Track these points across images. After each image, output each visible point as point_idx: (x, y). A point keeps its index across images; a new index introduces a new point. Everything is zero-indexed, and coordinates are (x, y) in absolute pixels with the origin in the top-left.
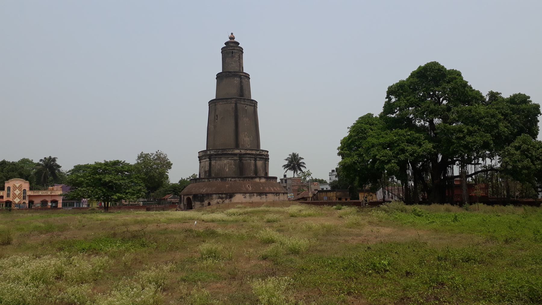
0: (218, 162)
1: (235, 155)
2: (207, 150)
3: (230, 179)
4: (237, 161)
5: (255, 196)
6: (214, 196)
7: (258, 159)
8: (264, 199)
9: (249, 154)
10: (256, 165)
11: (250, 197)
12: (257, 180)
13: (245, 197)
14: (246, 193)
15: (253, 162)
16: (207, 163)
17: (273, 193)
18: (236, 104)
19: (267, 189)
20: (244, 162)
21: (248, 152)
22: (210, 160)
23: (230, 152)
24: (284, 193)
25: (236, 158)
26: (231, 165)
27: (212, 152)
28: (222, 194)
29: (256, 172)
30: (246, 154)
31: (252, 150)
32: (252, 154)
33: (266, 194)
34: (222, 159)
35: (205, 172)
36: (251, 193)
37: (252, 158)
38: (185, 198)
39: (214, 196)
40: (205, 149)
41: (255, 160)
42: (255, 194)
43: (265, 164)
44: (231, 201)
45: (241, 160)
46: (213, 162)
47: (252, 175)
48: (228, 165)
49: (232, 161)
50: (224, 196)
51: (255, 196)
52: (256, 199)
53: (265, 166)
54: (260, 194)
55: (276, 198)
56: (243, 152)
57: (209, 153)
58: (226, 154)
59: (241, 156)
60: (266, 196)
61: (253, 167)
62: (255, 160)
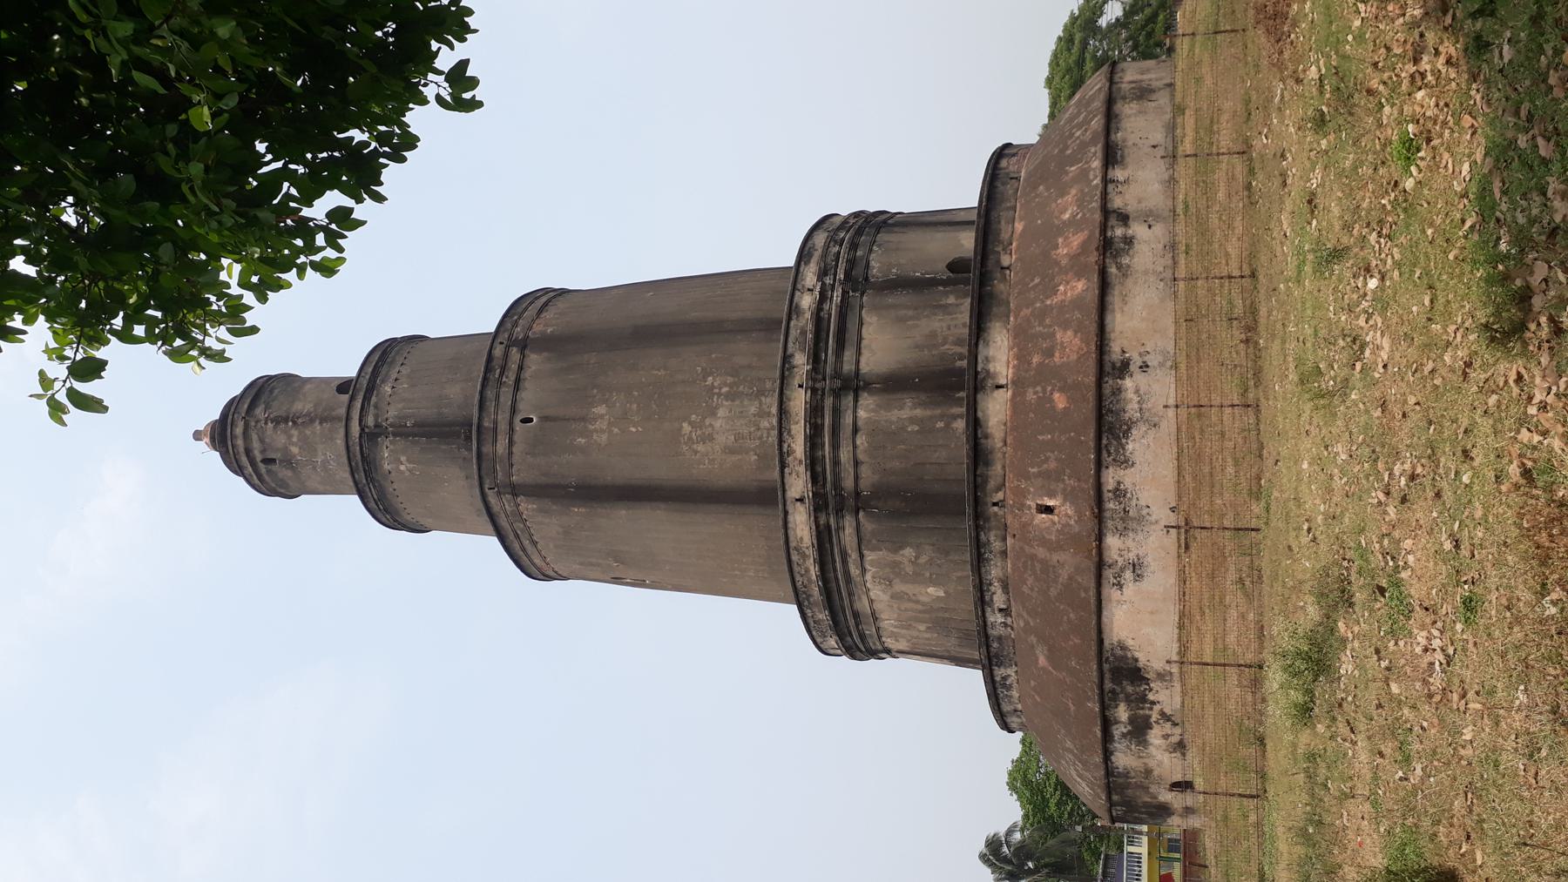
1: (824, 538)
3: (995, 618)
4: (868, 526)
5: (1128, 478)
6: (1124, 759)
7: (848, 367)
8: (1150, 392)
9: (813, 441)
10: (894, 384)
11: (1130, 522)
13: (1137, 567)
14: (1101, 565)
15: (867, 409)
17: (1104, 286)
18: (515, 490)
19: (1071, 344)
20: (868, 477)
21: (798, 446)
23: (814, 571)
24: (1112, 156)
25: (848, 536)
26: (895, 565)
28: (1107, 724)
30: (813, 463)
31: (783, 412)
32: (814, 411)
33: (1108, 369)
34: (863, 605)
36: (1101, 509)
37: (837, 413)
39: (1124, 759)
41: (854, 385)
42: (1110, 477)
44: (1161, 676)
45: (860, 502)
48: (899, 587)
49: (870, 556)
50: (1122, 713)
51: (1128, 478)
52: (1148, 471)
54: (1107, 428)
55: (1147, 243)
56: (798, 484)
58: (827, 592)
59: (829, 500)
60: (1123, 368)
61: (907, 412)
62: (854, 385)
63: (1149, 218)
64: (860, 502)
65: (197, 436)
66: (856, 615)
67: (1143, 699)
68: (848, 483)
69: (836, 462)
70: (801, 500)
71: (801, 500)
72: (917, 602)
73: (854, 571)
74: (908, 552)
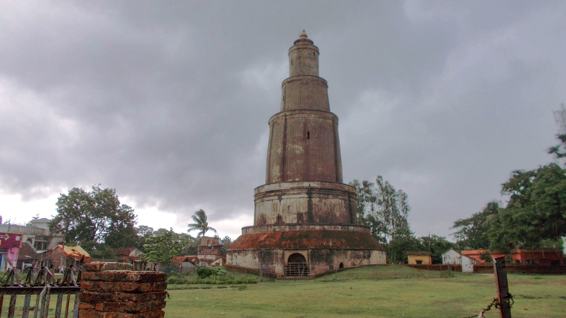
0: (323, 201)
22: (310, 197)
27: (313, 185)
34: (331, 196)
38: (288, 254)
46: (315, 200)
48: (338, 207)
65: (304, 31)
66: (328, 195)
67: (364, 257)
72: (334, 209)
73: (340, 197)
74: (345, 210)
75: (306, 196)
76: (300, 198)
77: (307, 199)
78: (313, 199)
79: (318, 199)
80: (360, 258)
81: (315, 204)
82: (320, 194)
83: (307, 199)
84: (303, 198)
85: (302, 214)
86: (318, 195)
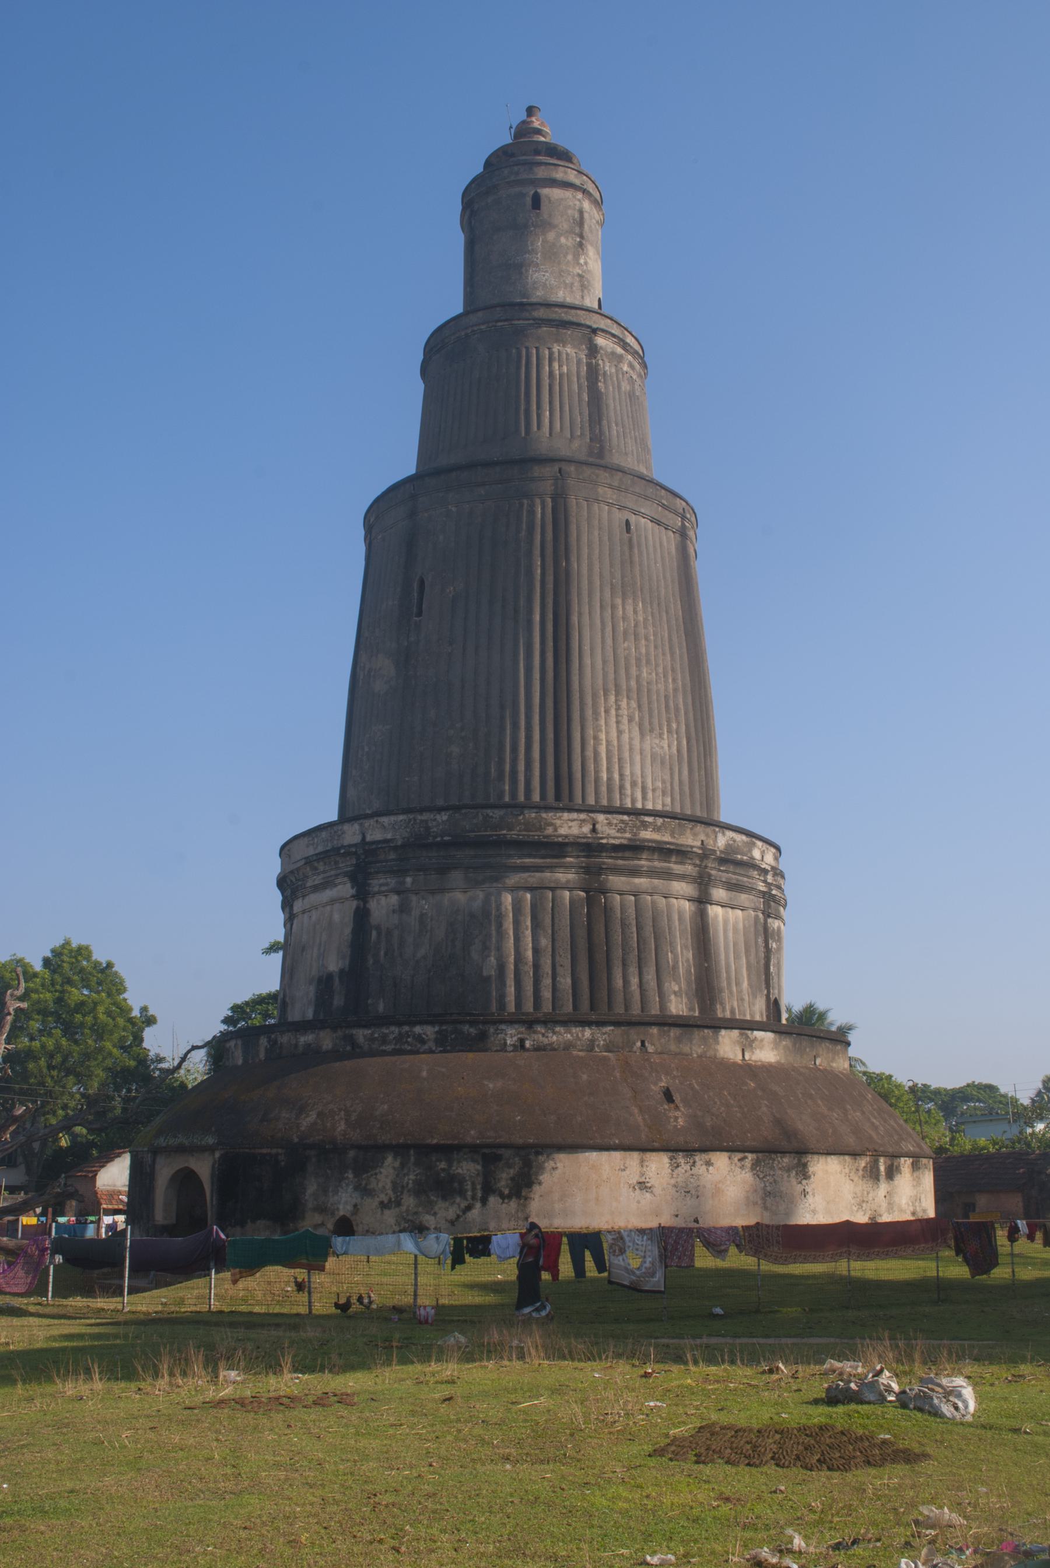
0: (421, 905)
2: (347, 814)
7: (719, 893)
12: (728, 1046)
16: (342, 916)
22: (362, 894)
29: (706, 985)
30: (635, 848)
34: (456, 877)
35: (325, 983)
37: (682, 877)
40: (333, 816)
41: (702, 901)
43: (767, 934)
46: (382, 907)
47: (678, 1006)
53: (768, 951)
57: (351, 835)
61: (682, 954)
63: (889, 1195)
64: (594, 890)
66: (443, 870)
68: (616, 881)
69: (635, 872)
70: (594, 830)
71: (594, 830)
75: (345, 889)
76: (332, 902)
77: (355, 903)
78: (372, 905)
79: (394, 899)
80: (462, 1193)
81: (378, 928)
82: (401, 872)
83: (355, 903)
84: (340, 900)
85: (330, 977)
86: (392, 881)
